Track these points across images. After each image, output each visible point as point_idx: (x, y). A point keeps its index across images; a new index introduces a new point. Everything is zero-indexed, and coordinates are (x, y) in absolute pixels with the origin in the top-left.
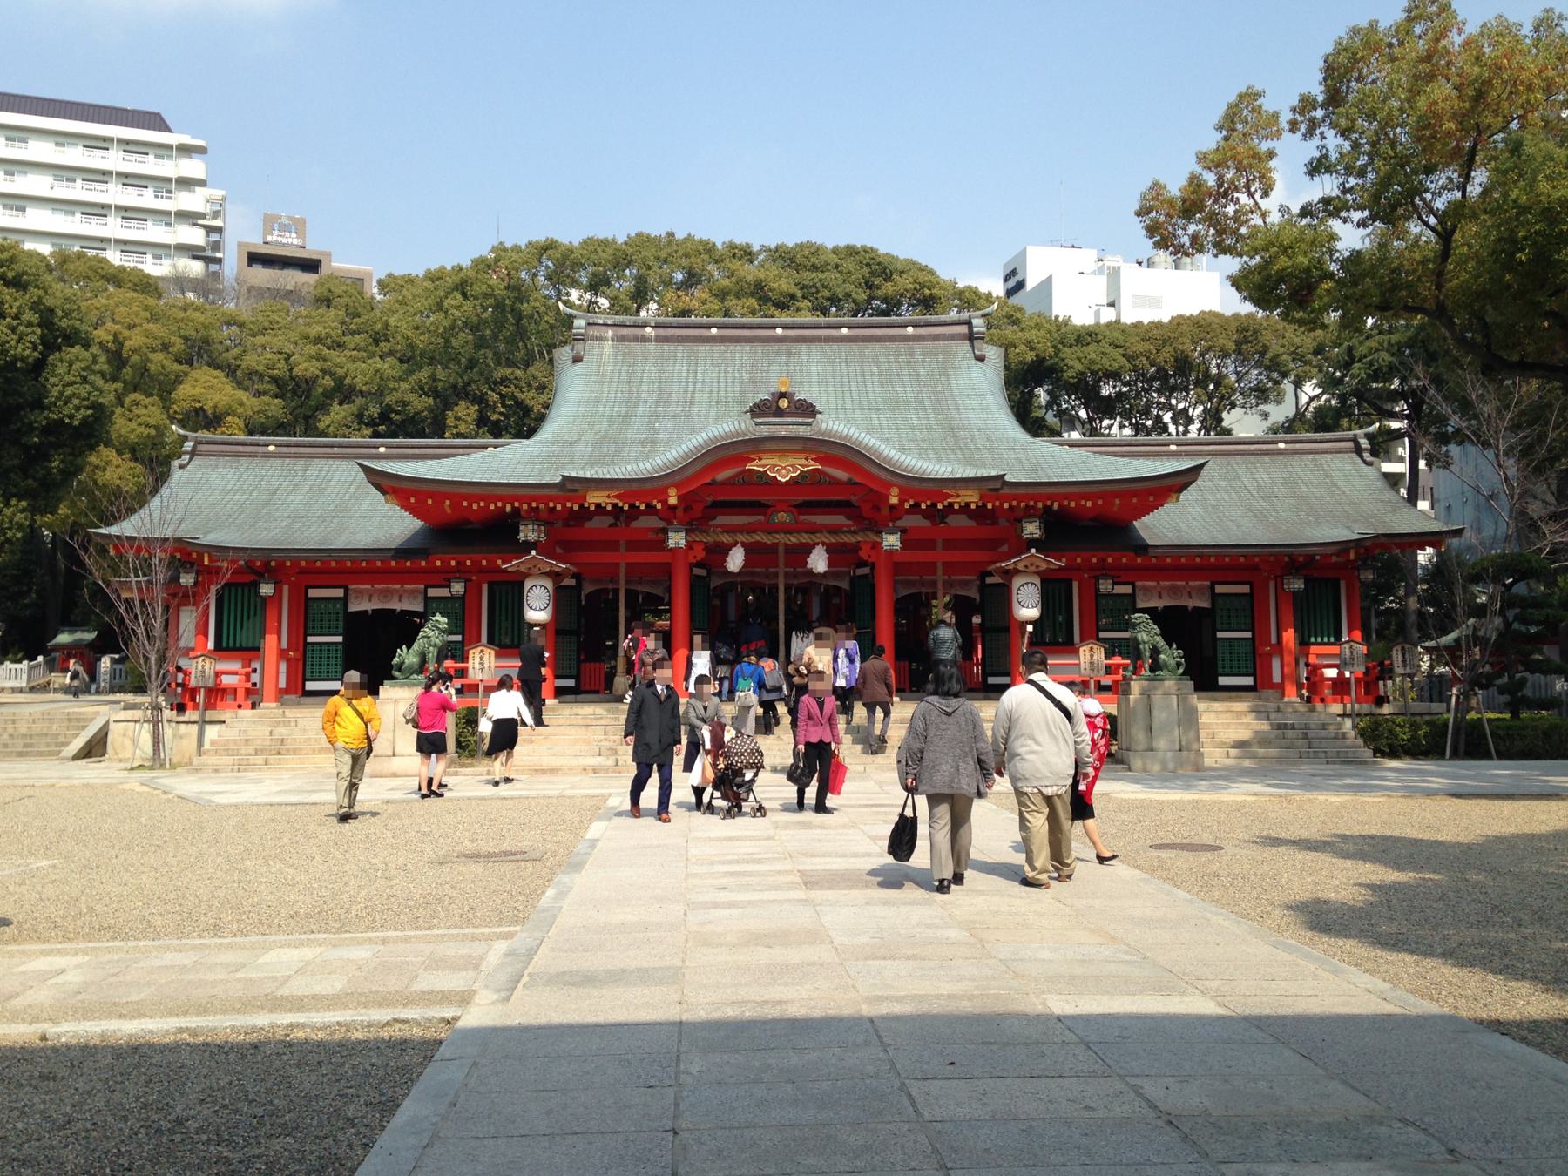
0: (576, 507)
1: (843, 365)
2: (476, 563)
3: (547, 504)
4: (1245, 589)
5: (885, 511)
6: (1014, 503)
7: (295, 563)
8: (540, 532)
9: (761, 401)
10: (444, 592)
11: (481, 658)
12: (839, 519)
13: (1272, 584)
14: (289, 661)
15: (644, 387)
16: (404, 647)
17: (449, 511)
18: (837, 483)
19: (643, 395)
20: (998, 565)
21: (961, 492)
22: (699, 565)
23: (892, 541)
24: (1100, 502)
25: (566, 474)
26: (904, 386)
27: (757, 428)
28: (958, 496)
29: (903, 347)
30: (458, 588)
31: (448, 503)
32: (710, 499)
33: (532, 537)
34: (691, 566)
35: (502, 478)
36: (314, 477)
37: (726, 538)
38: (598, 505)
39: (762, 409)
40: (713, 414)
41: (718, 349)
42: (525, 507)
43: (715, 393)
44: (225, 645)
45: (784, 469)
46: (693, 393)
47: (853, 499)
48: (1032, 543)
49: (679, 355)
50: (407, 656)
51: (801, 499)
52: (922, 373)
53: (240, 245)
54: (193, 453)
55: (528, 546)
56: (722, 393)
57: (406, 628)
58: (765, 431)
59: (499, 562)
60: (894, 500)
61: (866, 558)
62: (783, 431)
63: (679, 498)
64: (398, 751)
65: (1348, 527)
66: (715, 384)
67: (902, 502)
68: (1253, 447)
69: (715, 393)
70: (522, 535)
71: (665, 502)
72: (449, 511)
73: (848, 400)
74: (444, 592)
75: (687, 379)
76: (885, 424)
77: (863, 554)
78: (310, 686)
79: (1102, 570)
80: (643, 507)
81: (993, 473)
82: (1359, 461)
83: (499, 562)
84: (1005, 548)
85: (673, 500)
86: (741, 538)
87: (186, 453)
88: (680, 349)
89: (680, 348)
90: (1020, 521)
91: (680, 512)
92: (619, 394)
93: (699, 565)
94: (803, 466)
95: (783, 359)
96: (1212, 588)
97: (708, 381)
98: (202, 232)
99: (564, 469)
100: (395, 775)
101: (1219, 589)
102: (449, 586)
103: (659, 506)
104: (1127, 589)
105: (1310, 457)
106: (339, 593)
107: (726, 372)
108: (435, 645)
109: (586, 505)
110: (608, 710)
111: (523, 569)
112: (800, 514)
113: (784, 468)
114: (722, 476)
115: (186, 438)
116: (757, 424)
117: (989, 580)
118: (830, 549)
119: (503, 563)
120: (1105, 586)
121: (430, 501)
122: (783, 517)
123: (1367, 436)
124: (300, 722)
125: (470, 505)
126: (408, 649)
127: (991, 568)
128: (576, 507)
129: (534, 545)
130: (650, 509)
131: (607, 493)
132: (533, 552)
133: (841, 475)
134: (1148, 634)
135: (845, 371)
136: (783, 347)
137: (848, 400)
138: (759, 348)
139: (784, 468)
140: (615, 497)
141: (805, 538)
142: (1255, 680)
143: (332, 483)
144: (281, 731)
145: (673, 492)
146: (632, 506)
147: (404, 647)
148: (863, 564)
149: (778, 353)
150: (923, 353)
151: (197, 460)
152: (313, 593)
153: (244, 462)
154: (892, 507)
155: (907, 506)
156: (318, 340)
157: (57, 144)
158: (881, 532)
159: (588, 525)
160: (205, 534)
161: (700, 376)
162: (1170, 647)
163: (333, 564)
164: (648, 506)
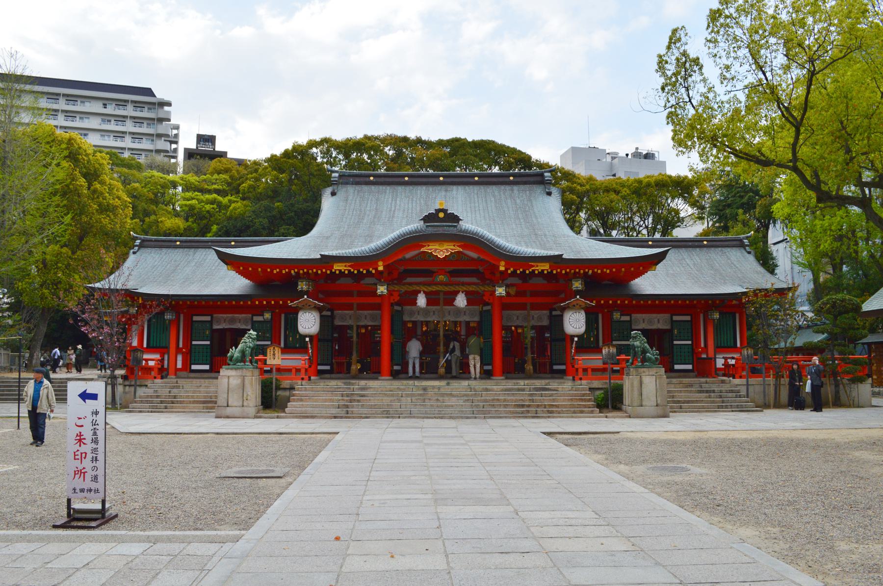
0: (328, 272)
1: (476, 196)
2: (277, 303)
3: (312, 271)
4: (688, 318)
5: (498, 275)
6: (568, 270)
7: (185, 303)
8: (309, 285)
9: (429, 213)
10: (260, 318)
11: (274, 352)
12: (474, 280)
13: (702, 316)
14: (183, 354)
15: (368, 209)
16: (234, 347)
17: (261, 274)
18: (473, 259)
19: (368, 213)
20: (558, 305)
21: (539, 264)
22: (398, 304)
23: (500, 291)
24: (614, 270)
25: (323, 253)
26: (508, 208)
27: (428, 229)
28: (537, 266)
29: (508, 188)
30: (268, 316)
31: (260, 270)
32: (402, 268)
33: (305, 288)
34: (392, 305)
35: (289, 256)
36: (198, 258)
38: (340, 271)
39: (428, 219)
40: (404, 223)
41: (408, 188)
42: (301, 272)
43: (406, 211)
44: (151, 345)
45: (441, 250)
46: (394, 211)
47: (481, 269)
48: (578, 292)
49: (388, 191)
50: (235, 352)
51: (451, 268)
52: (518, 201)
53: (186, 150)
54: (141, 246)
55: (302, 293)
56: (410, 211)
57: (237, 336)
58: (430, 230)
59: (289, 302)
60: (502, 268)
61: (487, 300)
62: (440, 231)
63: (384, 267)
64: (229, 404)
65: (740, 286)
66: (406, 207)
67: (507, 269)
68: (690, 244)
69: (406, 211)
70: (299, 287)
71: (376, 269)
72: (261, 274)
73: (478, 215)
74: (260, 318)
75: (391, 204)
76: (497, 227)
77: (486, 298)
78: (194, 367)
79: (615, 306)
80: (365, 272)
81: (557, 253)
82: (744, 251)
83: (289, 302)
84: (563, 296)
85: (381, 268)
87: (137, 246)
88: (388, 189)
89: (388, 188)
90: (571, 281)
91: (386, 275)
92: (355, 212)
94: (452, 249)
95: (443, 193)
96: (672, 318)
97: (402, 205)
98: (169, 143)
99: (322, 251)
100: (228, 417)
101: (675, 318)
102: (263, 315)
103: (374, 272)
104: (627, 318)
105: (720, 249)
107: (412, 200)
108: (250, 347)
109: (333, 271)
110: (345, 383)
111: (300, 306)
112: (452, 276)
113: (441, 251)
114: (409, 255)
115: (137, 238)
116: (427, 226)
117: (554, 313)
118: (467, 294)
119: (291, 303)
120: (616, 316)
121: (250, 269)
122: (441, 278)
123: (747, 238)
124: (185, 387)
125: (272, 271)
126: (236, 348)
127: (555, 306)
128: (328, 272)
129: (307, 293)
130: (369, 274)
131: (344, 264)
132: (306, 297)
133: (473, 255)
134: (639, 342)
135: (476, 199)
136: (444, 187)
137: (478, 215)
138: (431, 188)
139: (441, 251)
140: (349, 266)
141: (452, 289)
142: (693, 367)
143: (207, 260)
144: (175, 391)
145: (380, 263)
146: (359, 271)
147: (234, 347)
148: (487, 304)
149: (440, 190)
150: (518, 190)
151: (142, 250)
152: (195, 318)
153: (164, 250)
154: (502, 272)
155: (509, 272)
158: (494, 286)
159: (338, 282)
160: (141, 287)
161: (398, 202)
162: (652, 349)
163: (203, 303)
164: (368, 271)
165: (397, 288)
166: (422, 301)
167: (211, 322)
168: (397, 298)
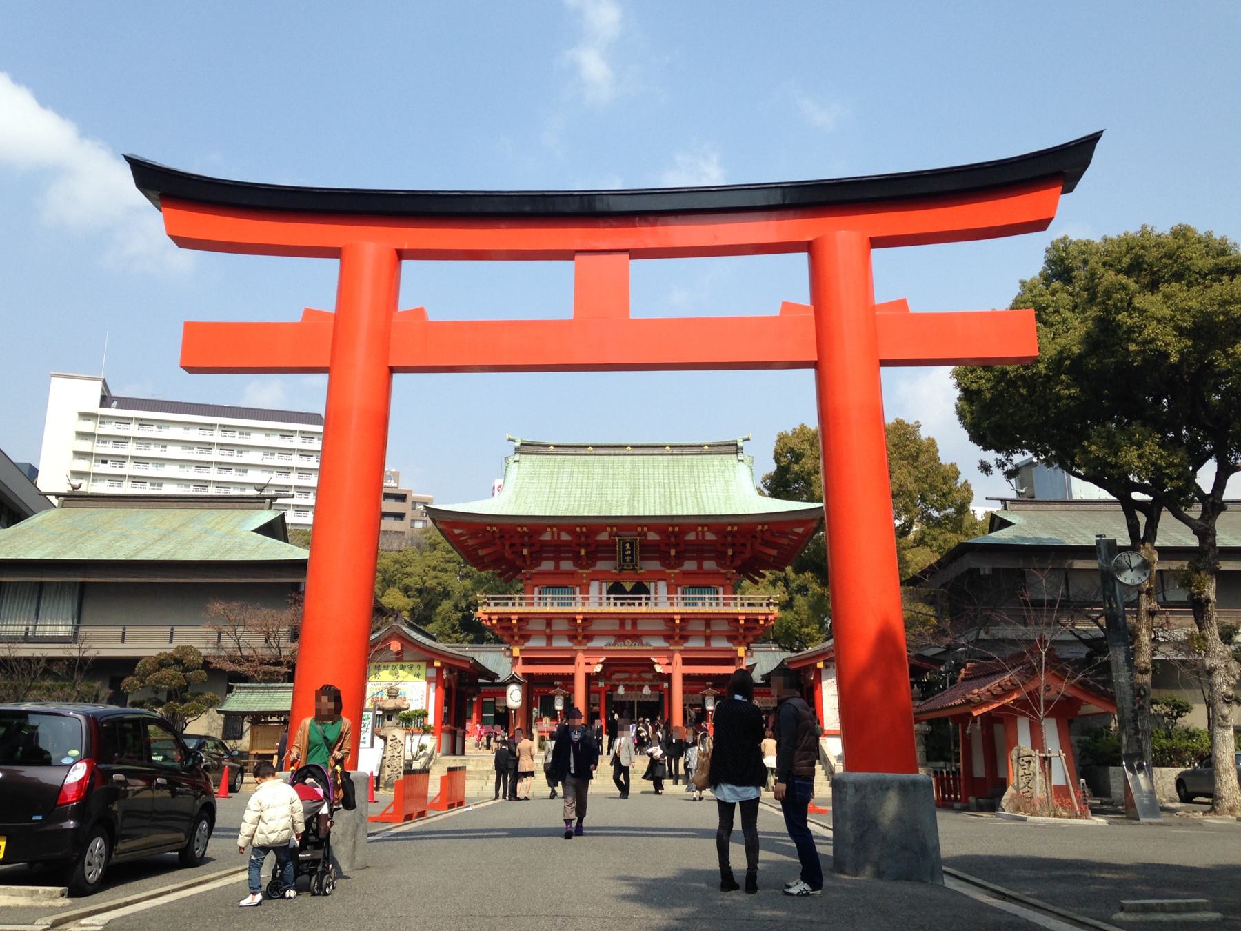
22: (610, 691)
37: (617, 683)
55: (556, 686)
86: (622, 683)
93: (610, 691)
106: (493, 699)
122: (635, 676)
141: (642, 683)
152: (485, 699)
156: (434, 569)
157: (266, 435)
165: (610, 683)
166: (621, 690)
167: (494, 702)
168: (609, 688)
